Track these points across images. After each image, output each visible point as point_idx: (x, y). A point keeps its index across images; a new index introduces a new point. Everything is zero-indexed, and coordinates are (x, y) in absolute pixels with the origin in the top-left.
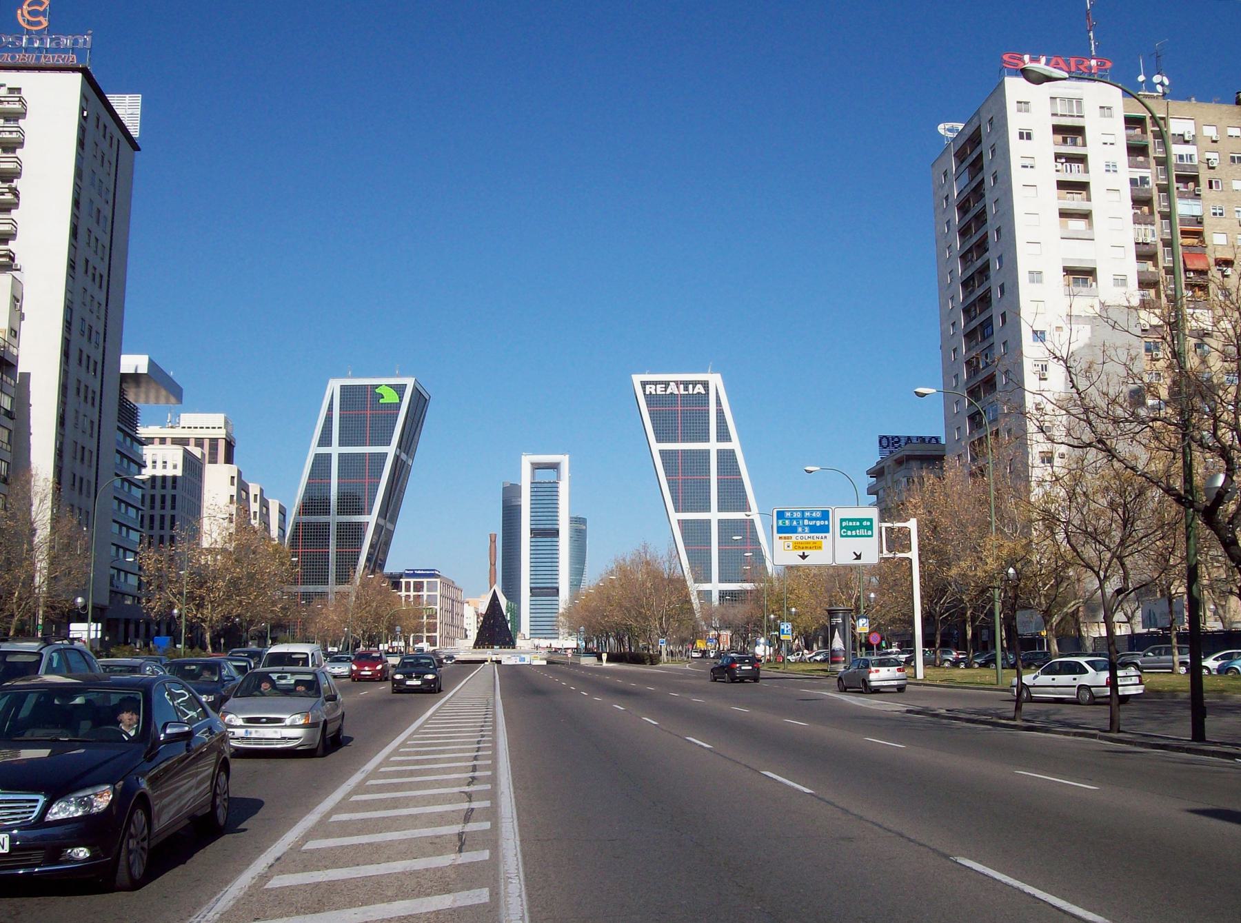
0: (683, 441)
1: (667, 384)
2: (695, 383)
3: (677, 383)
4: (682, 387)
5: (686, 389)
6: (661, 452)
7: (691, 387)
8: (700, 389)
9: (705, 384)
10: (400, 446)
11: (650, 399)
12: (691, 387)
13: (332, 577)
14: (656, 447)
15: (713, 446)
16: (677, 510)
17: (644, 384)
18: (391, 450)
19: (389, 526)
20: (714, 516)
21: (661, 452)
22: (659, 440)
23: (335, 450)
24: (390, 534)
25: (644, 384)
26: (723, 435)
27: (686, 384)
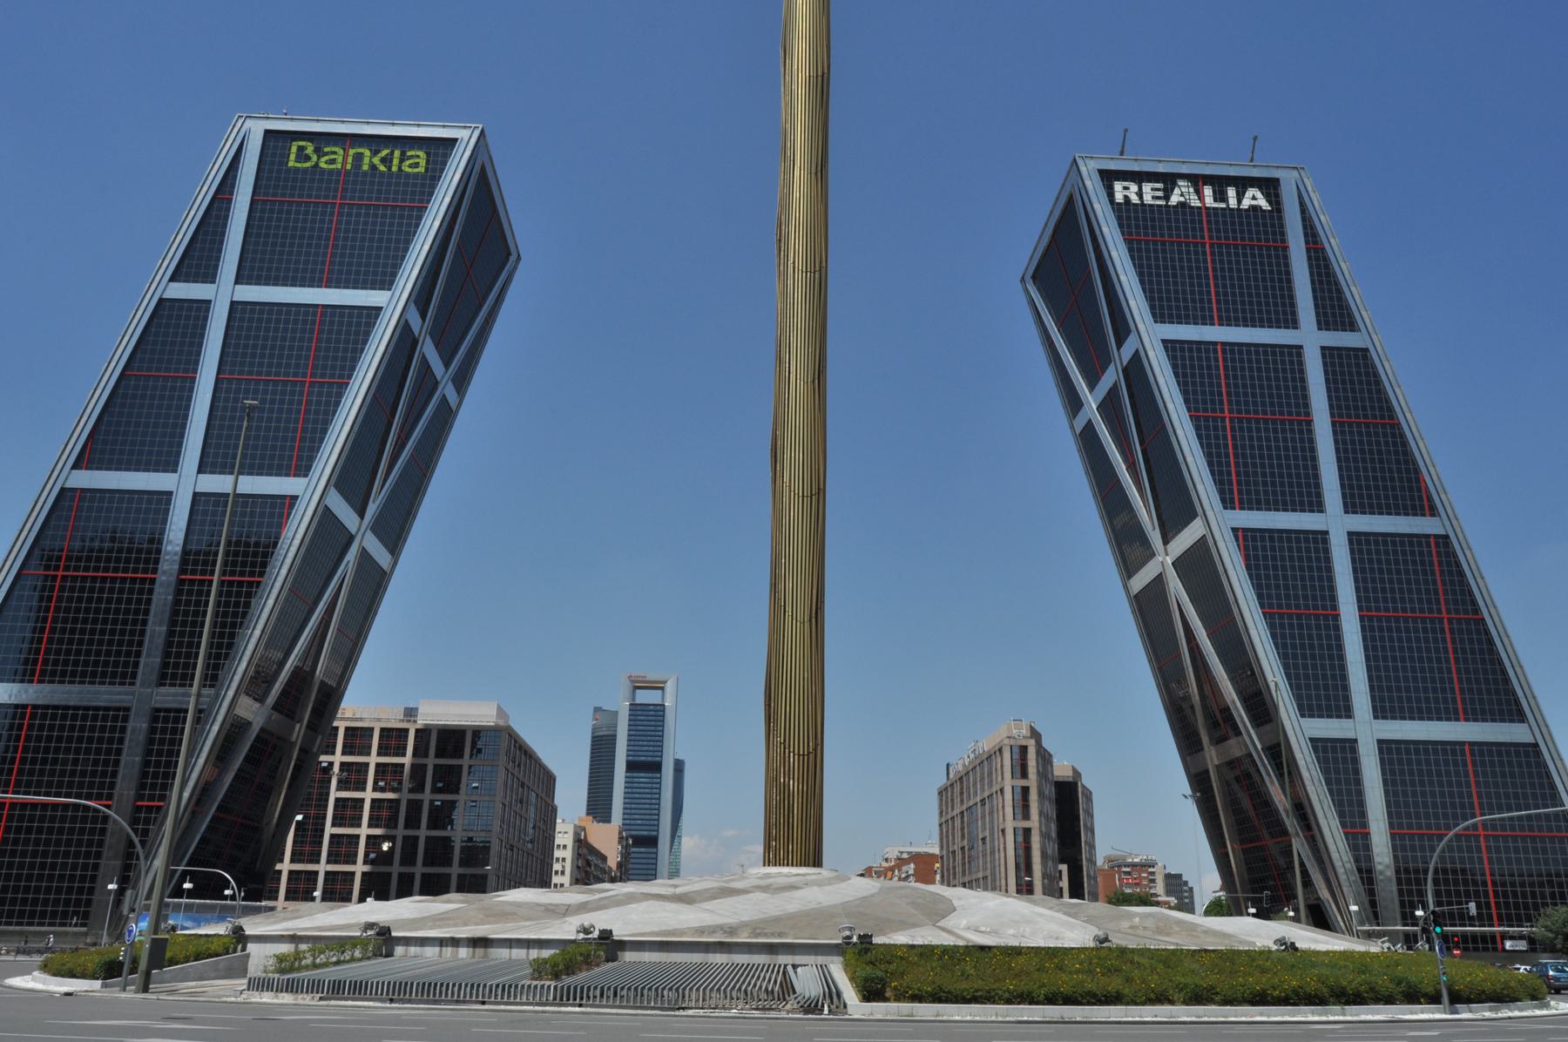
0: (1226, 321)
1: (1169, 181)
2: (1242, 184)
3: (1197, 181)
5: (1220, 196)
7: (1231, 192)
8: (1255, 198)
9: (1270, 186)
10: (421, 297)
11: (1126, 214)
12: (1231, 192)
13: (150, 660)
14: (1151, 336)
15: (1310, 338)
16: (1228, 503)
17: (1108, 177)
18: (391, 303)
19: (381, 556)
20: (1336, 522)
22: (1160, 315)
23: (223, 292)
24: (373, 582)
25: (1108, 177)
26: (1334, 312)
27: (1220, 184)
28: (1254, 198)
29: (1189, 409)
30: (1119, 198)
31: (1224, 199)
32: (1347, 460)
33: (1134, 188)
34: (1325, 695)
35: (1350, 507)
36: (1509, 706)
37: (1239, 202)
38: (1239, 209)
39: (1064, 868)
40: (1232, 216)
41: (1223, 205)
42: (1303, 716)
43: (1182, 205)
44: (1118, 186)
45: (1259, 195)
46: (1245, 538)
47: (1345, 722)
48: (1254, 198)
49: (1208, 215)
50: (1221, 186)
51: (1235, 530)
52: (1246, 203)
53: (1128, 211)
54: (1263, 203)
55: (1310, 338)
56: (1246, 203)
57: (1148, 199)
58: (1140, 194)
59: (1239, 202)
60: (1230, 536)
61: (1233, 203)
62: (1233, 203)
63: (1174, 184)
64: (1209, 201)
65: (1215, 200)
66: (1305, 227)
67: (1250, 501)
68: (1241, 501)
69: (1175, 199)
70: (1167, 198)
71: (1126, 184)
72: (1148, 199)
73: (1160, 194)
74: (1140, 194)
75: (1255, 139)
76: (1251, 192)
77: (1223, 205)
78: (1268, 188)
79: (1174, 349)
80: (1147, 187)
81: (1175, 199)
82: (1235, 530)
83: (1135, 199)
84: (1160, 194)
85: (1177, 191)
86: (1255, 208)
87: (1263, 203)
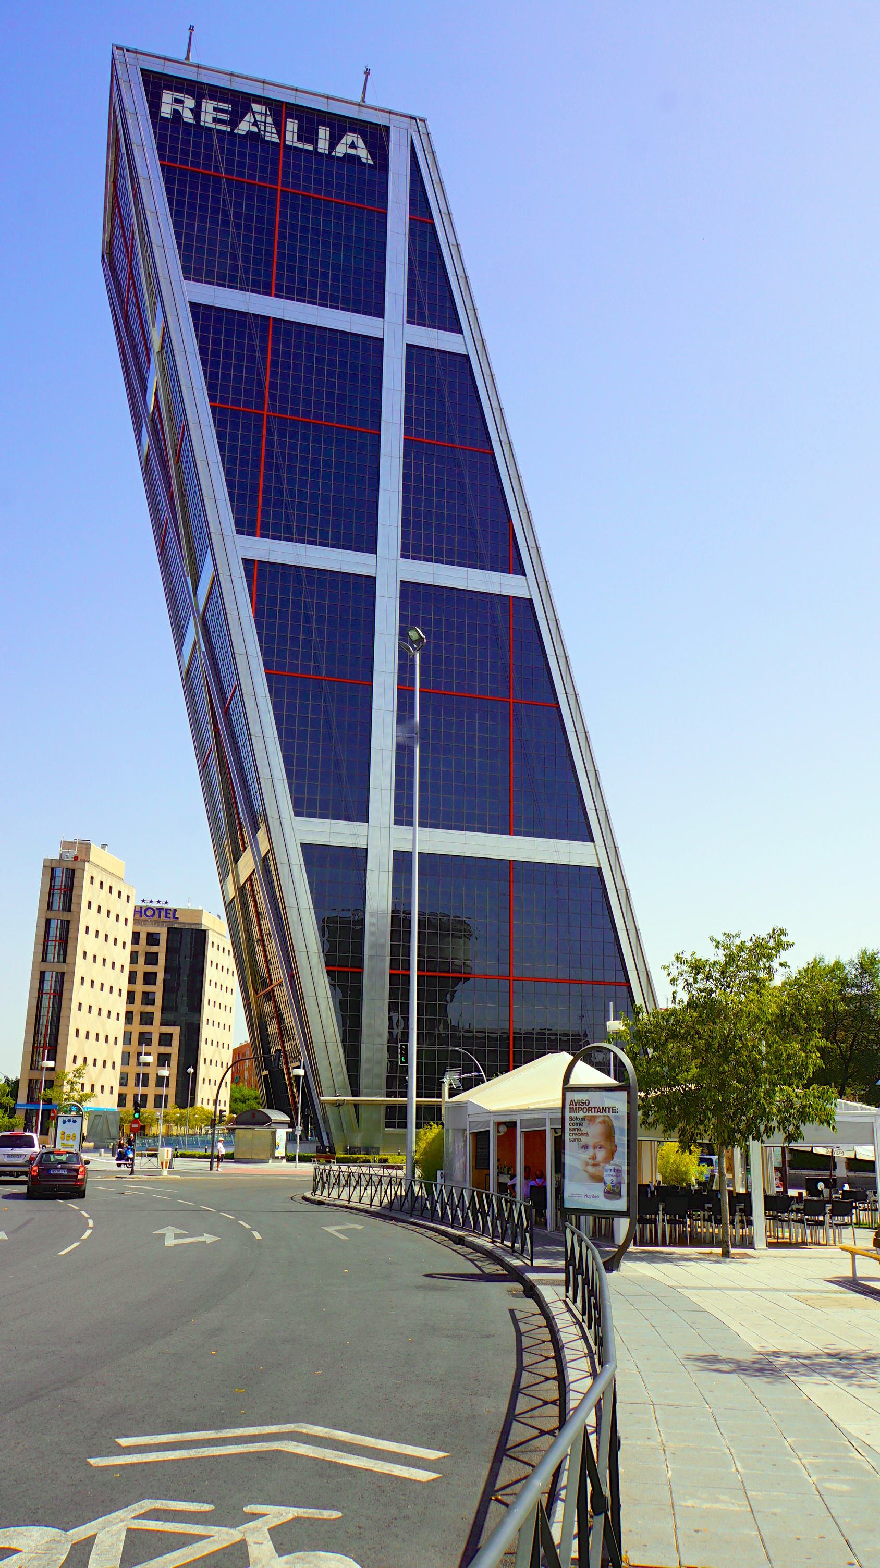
1: (239, 103)
2: (340, 126)
3: (280, 111)
4: (292, 126)
6: (202, 314)
7: (323, 133)
9: (376, 136)
12: (323, 133)
15: (396, 331)
16: (245, 526)
17: (155, 84)
20: (389, 567)
21: (202, 314)
22: (192, 272)
25: (155, 84)
27: (310, 119)
28: (353, 146)
29: (212, 398)
30: (166, 110)
31: (314, 141)
32: (418, 491)
33: (190, 103)
34: (330, 783)
35: (410, 550)
36: (568, 814)
37: (332, 146)
38: (329, 156)
39: (175, 1031)
40: (319, 163)
41: (310, 147)
42: (297, 814)
43: (254, 138)
44: (167, 97)
45: (360, 143)
46: (261, 576)
47: (359, 827)
48: (353, 146)
49: (287, 155)
50: (310, 121)
51: (246, 562)
52: (341, 150)
53: (175, 130)
54: (363, 153)
55: (396, 331)
56: (341, 150)
57: (207, 119)
58: (197, 112)
59: (332, 146)
60: (239, 571)
61: (323, 145)
62: (323, 145)
63: (248, 109)
64: (291, 138)
65: (300, 139)
66: (412, 192)
67: (276, 527)
68: (265, 526)
69: (244, 127)
70: (234, 123)
71: (179, 96)
72: (207, 119)
73: (225, 117)
74: (197, 112)
75: (367, 73)
76: (349, 138)
77: (310, 147)
78: (373, 136)
79: (207, 318)
80: (208, 106)
81: (244, 127)
82: (246, 562)
83: (188, 116)
84: (225, 117)
85: (249, 117)
86: (352, 159)
87: (363, 153)
